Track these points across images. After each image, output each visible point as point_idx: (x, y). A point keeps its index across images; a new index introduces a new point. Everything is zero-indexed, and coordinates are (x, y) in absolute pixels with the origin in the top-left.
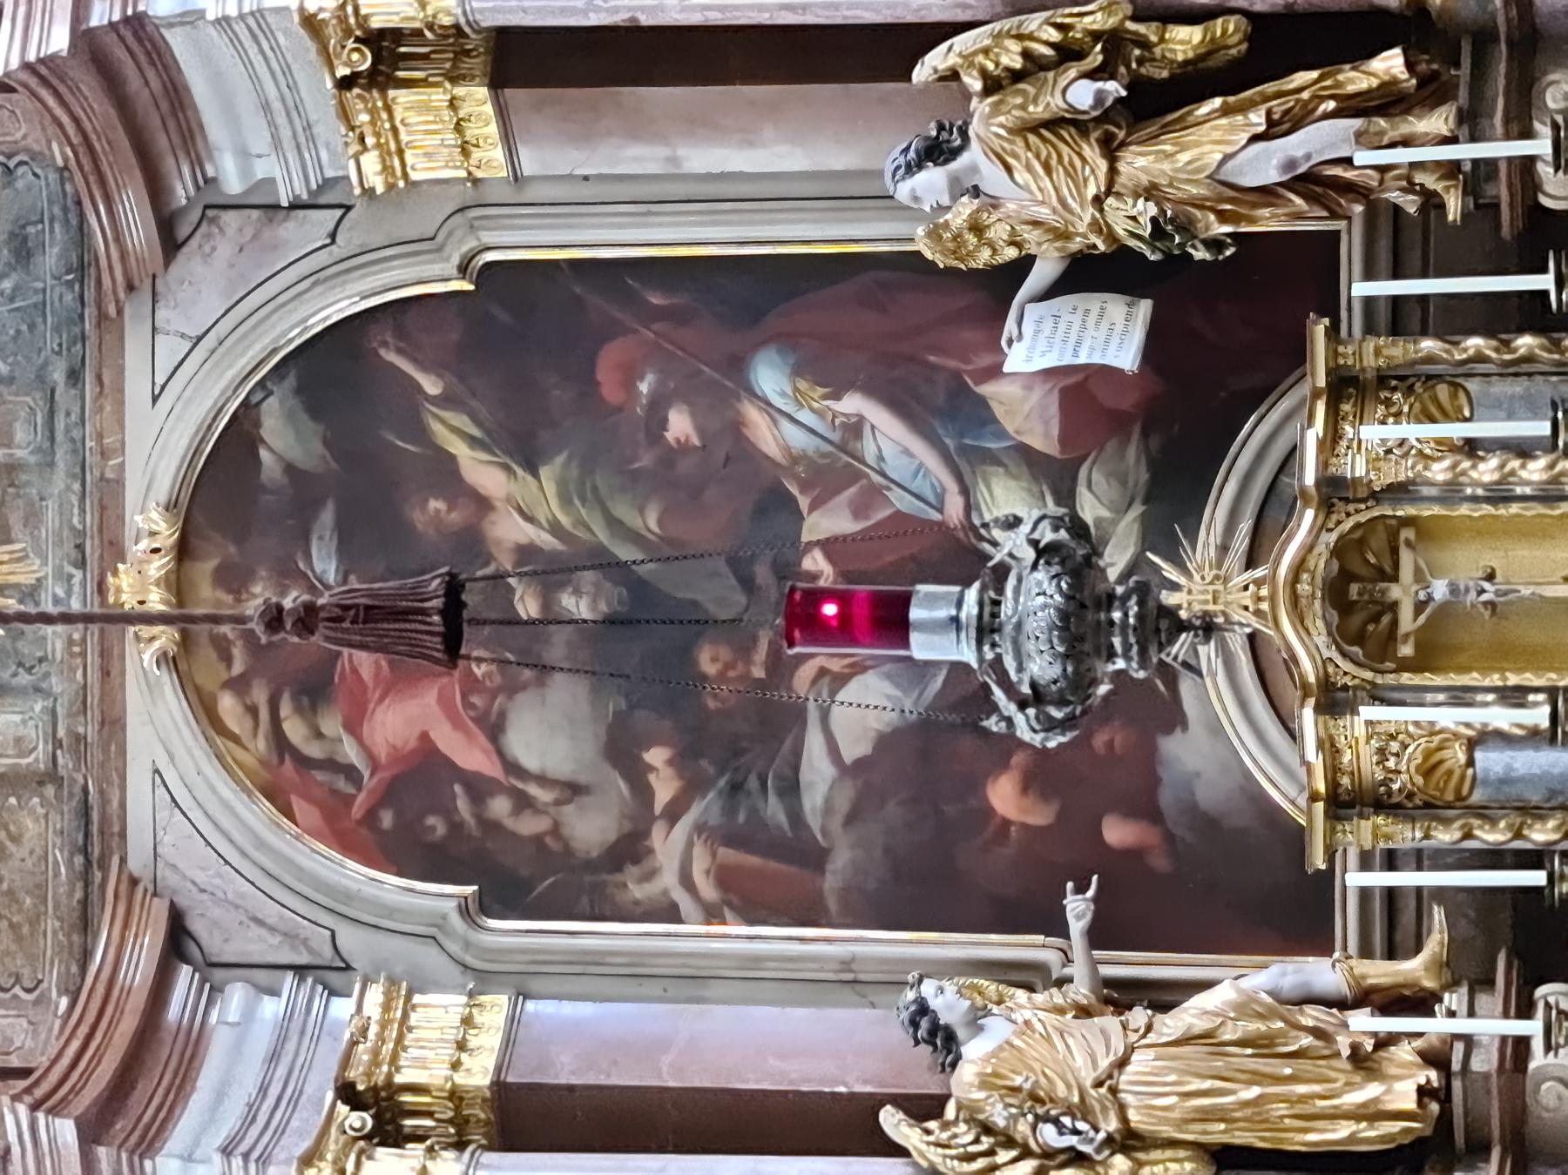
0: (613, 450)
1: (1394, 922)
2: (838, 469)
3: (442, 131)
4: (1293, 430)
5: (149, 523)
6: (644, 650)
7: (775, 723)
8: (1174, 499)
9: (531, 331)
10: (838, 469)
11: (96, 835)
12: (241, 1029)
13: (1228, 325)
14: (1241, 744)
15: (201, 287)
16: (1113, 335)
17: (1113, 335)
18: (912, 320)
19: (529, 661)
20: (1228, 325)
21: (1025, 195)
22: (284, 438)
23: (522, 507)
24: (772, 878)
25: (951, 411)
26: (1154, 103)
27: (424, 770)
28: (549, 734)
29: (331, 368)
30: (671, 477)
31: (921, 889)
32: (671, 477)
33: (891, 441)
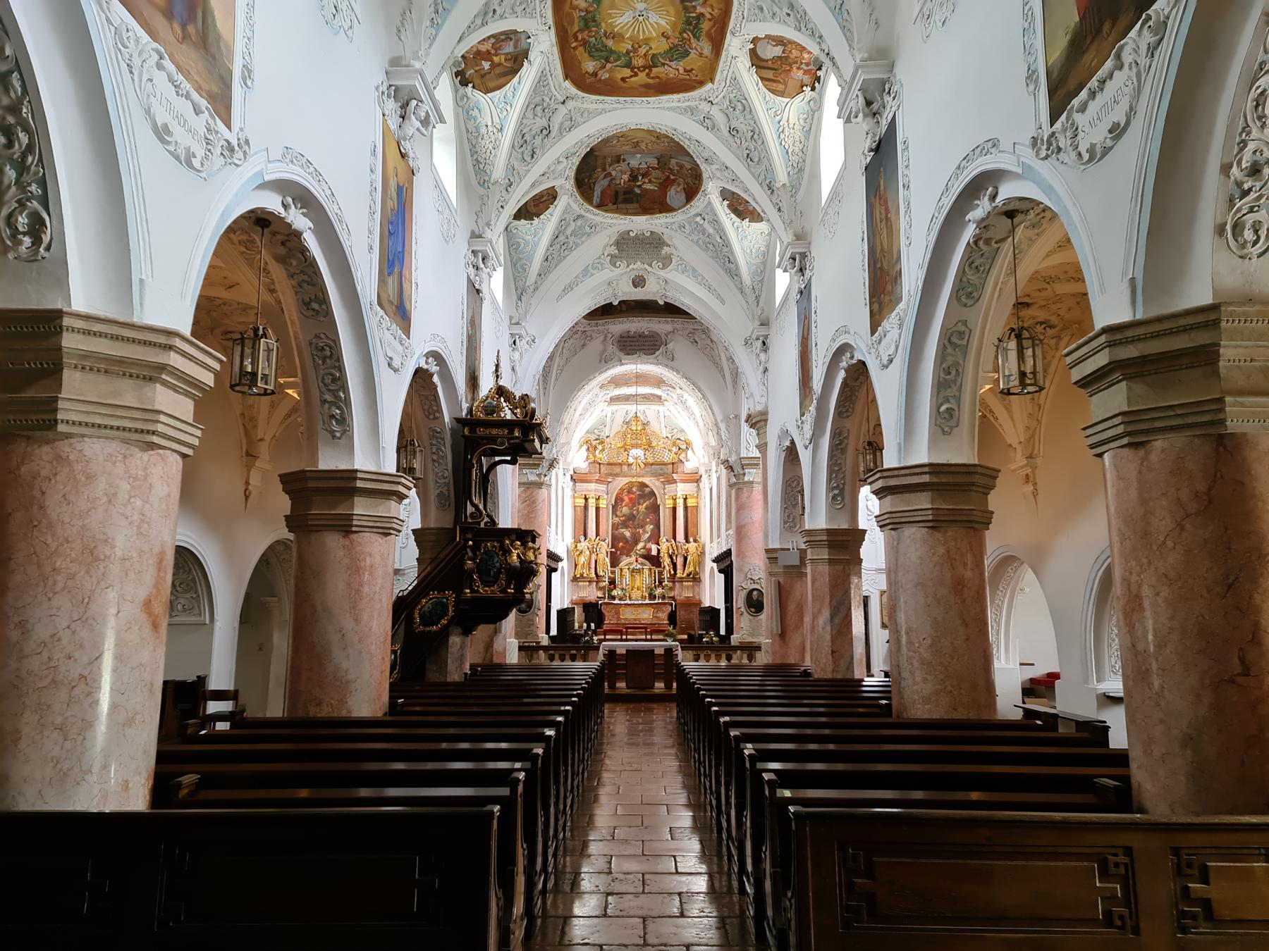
0: (646, 515)
1: (613, 572)
2: (645, 532)
3: (669, 503)
4: (648, 566)
5: (640, 480)
6: (631, 517)
7: (627, 527)
8: (644, 557)
9: (655, 509)
10: (645, 532)
11: (617, 475)
12: (603, 487)
13: (655, 561)
14: (625, 561)
15: (658, 483)
16: (654, 553)
17: (654, 553)
18: (655, 537)
19: (631, 509)
20: (655, 561)
21: (664, 546)
22: (647, 490)
23: (642, 508)
24: (615, 527)
25: (649, 540)
26: (671, 557)
27: (623, 500)
28: (625, 510)
29: (652, 494)
30: (644, 520)
31: (615, 540)
32: (644, 520)
33: (647, 536)
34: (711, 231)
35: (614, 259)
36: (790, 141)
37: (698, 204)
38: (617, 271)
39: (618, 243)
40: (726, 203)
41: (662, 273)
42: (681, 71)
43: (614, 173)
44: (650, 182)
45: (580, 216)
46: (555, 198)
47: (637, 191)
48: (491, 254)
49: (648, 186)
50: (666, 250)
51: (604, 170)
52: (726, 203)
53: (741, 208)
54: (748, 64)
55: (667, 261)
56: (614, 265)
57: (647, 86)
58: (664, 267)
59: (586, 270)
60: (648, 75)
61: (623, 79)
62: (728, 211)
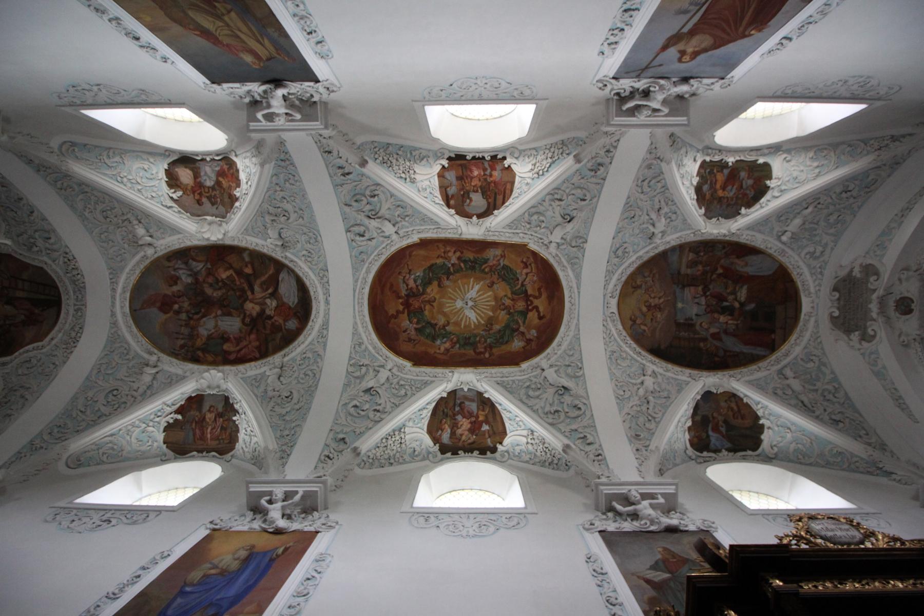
34: (798, 221)
35: (866, 338)
36: (544, 162)
37: (758, 240)
38: (882, 334)
39: (848, 331)
40: (743, 211)
41: (885, 276)
42: (525, 271)
43: (713, 330)
44: (734, 293)
45: (780, 372)
46: (734, 395)
47: (752, 306)
48: (623, 490)
49: (743, 294)
50: (857, 273)
51: (704, 340)
52: (743, 211)
53: (751, 193)
54: (491, 218)
55: (870, 270)
56: (874, 337)
57: (550, 298)
58: (877, 273)
59: (877, 374)
60: (536, 298)
61: (540, 318)
62: (757, 206)
